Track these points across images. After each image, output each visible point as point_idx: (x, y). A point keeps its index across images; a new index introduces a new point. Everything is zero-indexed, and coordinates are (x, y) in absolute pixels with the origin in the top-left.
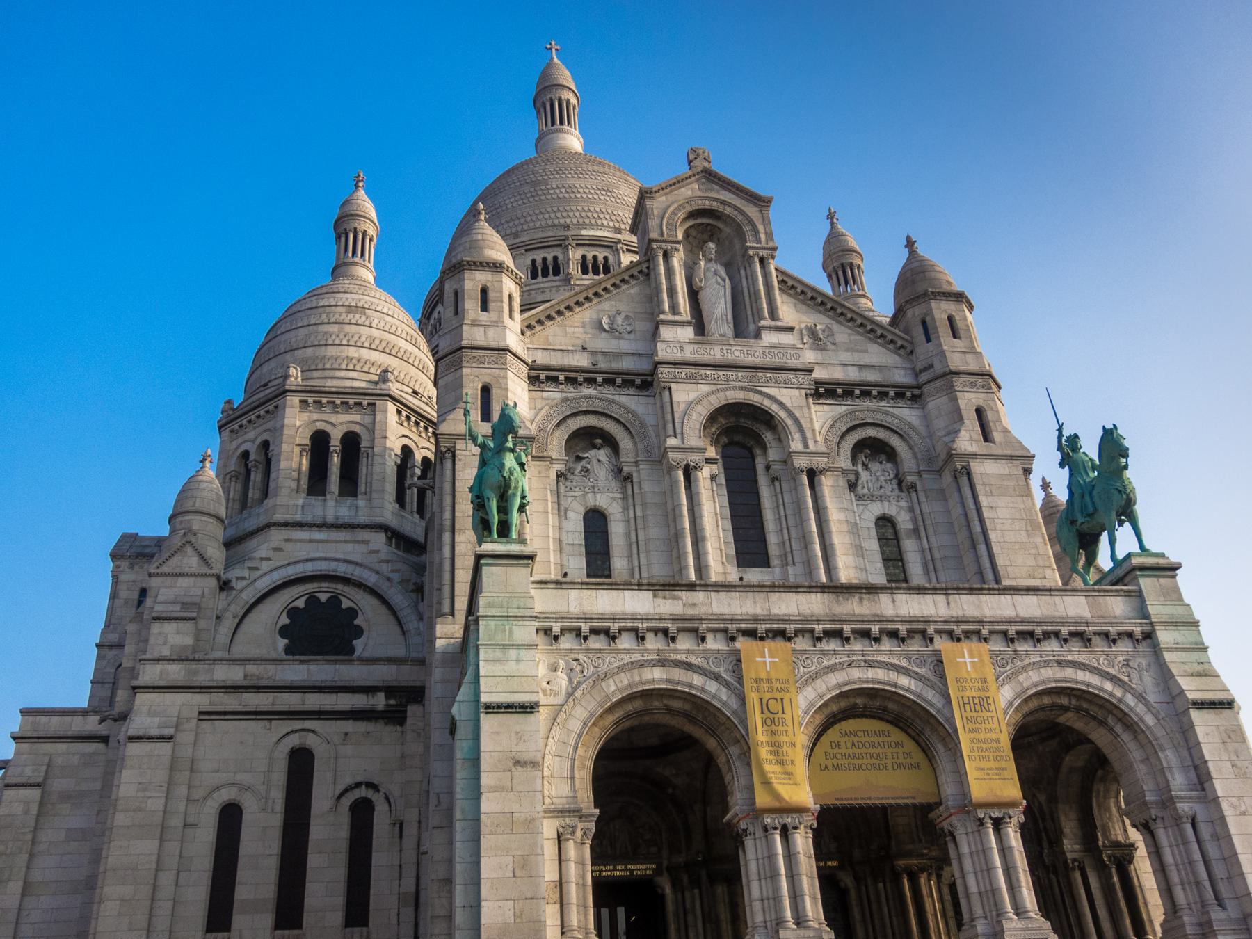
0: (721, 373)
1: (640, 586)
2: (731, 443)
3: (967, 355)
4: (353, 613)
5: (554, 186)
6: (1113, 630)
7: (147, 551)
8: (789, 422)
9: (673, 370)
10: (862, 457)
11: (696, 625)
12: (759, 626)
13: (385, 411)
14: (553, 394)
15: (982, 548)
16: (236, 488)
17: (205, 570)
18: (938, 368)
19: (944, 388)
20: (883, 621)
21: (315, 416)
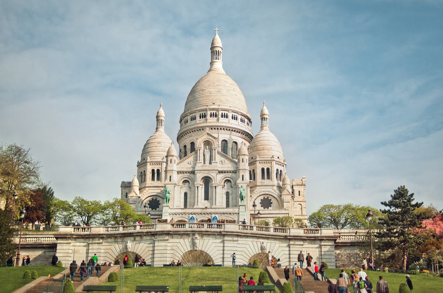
1: (180, 209)
2: (206, 181)
4: (159, 201)
5: (207, 92)
6: (234, 213)
7: (127, 185)
8: (213, 179)
10: (226, 182)
13: (164, 165)
14: (180, 175)
15: (238, 197)
16: (140, 178)
17: (136, 196)
21: (152, 166)
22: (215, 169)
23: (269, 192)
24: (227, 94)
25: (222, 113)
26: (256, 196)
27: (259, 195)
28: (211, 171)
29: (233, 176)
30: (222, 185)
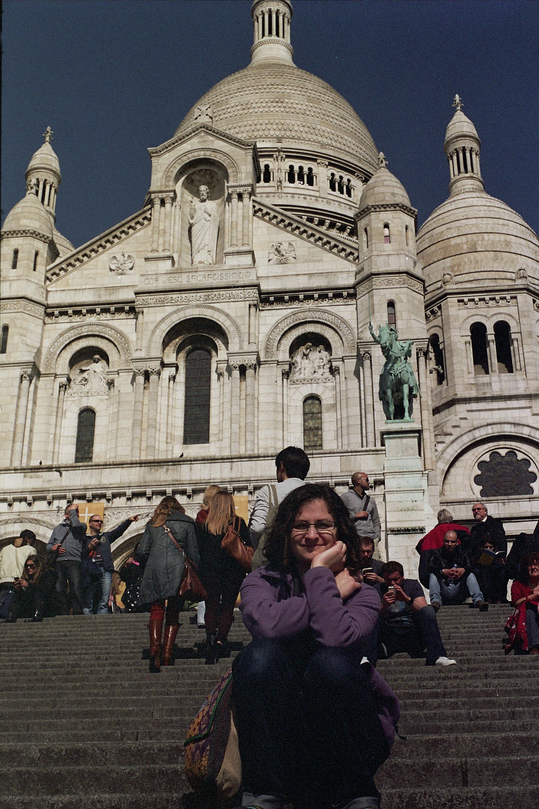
0: (184, 296)
3: (391, 257)
5: (232, 105)
9: (147, 297)
10: (303, 349)
11: (45, 495)
12: (88, 493)
18: (366, 272)
19: (367, 287)
20: (176, 484)
22: (241, 283)
23: (515, 424)
24: (310, 108)
25: (291, 167)
26: (457, 448)
27: (466, 440)
28: (222, 292)
29: (341, 314)
30: (278, 363)
